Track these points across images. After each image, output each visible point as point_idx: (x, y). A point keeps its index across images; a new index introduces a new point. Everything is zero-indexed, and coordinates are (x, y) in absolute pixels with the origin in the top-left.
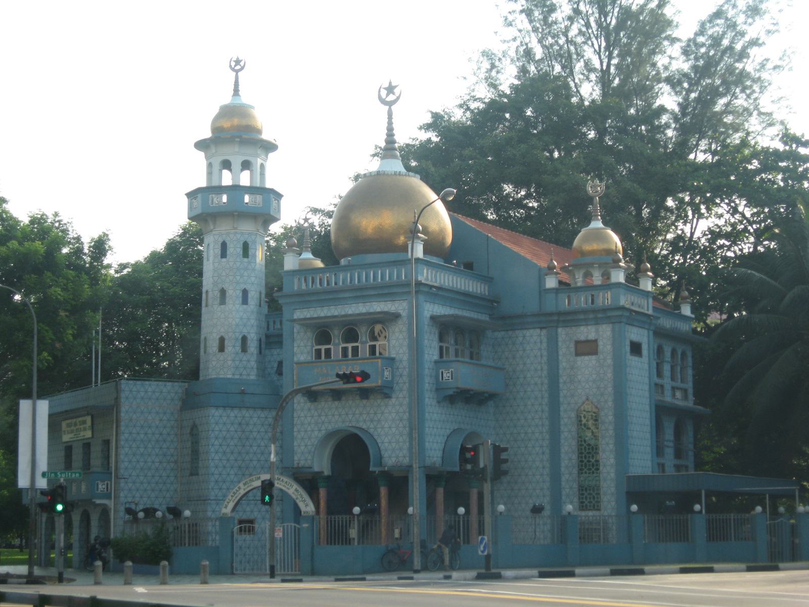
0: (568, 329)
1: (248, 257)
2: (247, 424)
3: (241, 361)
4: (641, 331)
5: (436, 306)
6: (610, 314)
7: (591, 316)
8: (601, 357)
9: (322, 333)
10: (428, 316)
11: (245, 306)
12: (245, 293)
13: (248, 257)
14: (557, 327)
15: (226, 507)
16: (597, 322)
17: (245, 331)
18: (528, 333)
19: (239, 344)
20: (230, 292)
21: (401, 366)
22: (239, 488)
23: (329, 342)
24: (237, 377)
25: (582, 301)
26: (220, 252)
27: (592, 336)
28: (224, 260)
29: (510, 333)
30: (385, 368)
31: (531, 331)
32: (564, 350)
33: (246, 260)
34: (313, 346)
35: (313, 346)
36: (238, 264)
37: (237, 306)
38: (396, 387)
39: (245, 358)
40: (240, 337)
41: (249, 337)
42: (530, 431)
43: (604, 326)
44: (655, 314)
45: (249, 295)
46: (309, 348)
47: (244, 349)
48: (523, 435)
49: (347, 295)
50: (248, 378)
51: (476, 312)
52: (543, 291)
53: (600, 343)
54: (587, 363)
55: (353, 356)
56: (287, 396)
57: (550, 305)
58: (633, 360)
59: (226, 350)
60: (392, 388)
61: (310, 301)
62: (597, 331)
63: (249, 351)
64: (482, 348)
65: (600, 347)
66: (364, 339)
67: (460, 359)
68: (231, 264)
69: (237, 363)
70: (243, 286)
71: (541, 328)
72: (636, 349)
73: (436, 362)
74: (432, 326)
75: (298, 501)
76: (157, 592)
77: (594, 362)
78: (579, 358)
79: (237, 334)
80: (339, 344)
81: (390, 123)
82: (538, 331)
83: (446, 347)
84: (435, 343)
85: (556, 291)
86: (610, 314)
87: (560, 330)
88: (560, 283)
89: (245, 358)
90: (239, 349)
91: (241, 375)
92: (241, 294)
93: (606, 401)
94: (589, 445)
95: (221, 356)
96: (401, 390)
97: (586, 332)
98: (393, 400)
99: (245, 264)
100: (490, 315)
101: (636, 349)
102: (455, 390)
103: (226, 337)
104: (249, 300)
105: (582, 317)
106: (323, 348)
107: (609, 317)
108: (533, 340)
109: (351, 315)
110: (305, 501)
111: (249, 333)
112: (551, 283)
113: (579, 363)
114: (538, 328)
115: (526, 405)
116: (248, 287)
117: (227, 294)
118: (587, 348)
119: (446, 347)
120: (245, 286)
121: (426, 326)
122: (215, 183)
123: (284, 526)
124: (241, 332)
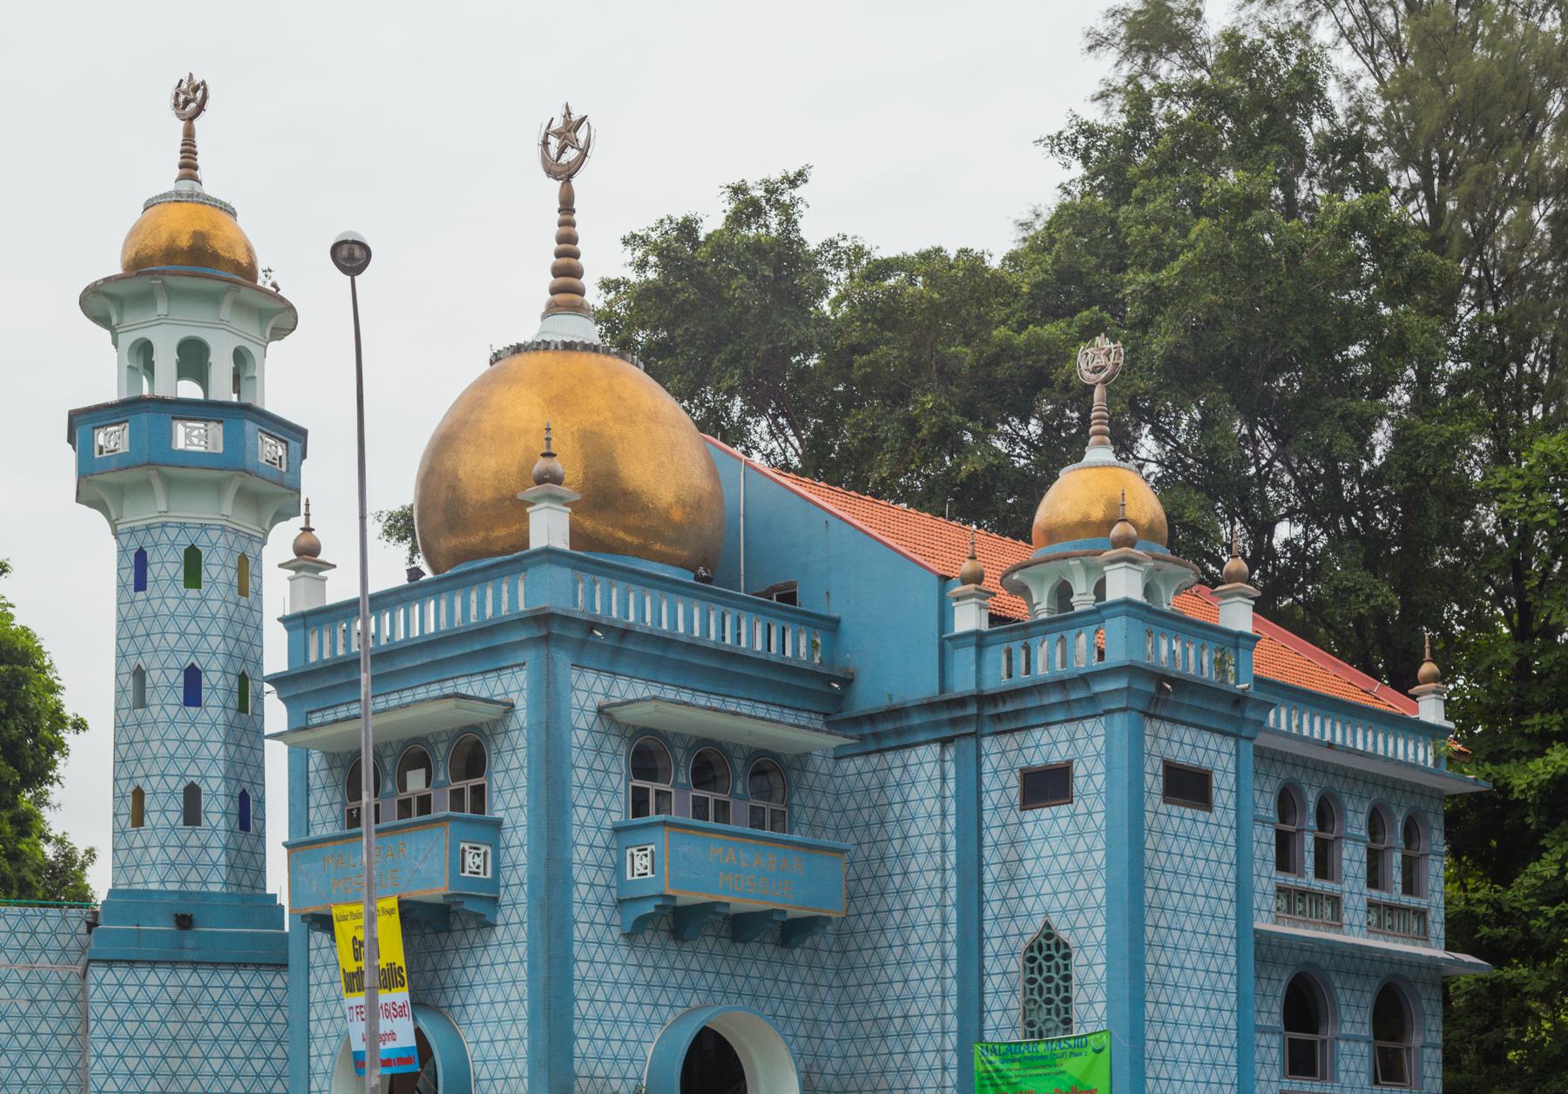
0: (1004, 739)
3: (183, 847)
4: (1213, 741)
5: (622, 683)
8: (1081, 809)
10: (591, 706)
11: (192, 710)
12: (193, 678)
14: (977, 736)
18: (913, 756)
20: (154, 676)
24: (170, 887)
25: (1046, 660)
26: (132, 578)
27: (1056, 758)
28: (141, 595)
29: (874, 759)
30: (467, 846)
33: (193, 593)
36: (172, 603)
37: (172, 710)
38: (505, 898)
40: (181, 787)
41: (204, 787)
42: (914, 1011)
44: (1259, 696)
45: (204, 681)
46: (337, 808)
47: (192, 812)
50: (204, 889)
51: (790, 708)
52: (948, 643)
53: (1079, 771)
54: (1049, 820)
57: (963, 682)
58: (1182, 817)
60: (496, 899)
62: (1072, 740)
63: (204, 822)
64: (796, 799)
65: (1079, 783)
66: (442, 778)
67: (767, 833)
69: (173, 852)
70: (186, 660)
71: (945, 742)
72: (1187, 786)
73: (617, 830)
74: (606, 733)
77: (1063, 822)
78: (1029, 816)
79: (172, 781)
81: (567, 243)
82: (936, 748)
83: (658, 793)
84: (615, 779)
85: (979, 640)
87: (987, 743)
88: (994, 619)
90: (175, 817)
91: (184, 882)
92: (181, 679)
97: (1047, 746)
98: (499, 930)
99: (193, 603)
100: (826, 715)
101: (1187, 786)
102: (659, 902)
103: (147, 789)
104: (205, 694)
108: (924, 776)
111: (203, 777)
112: (968, 618)
113: (1029, 827)
114: (935, 741)
115: (906, 945)
116: (201, 662)
117: (148, 681)
118: (1047, 786)
119: (658, 793)
120: (193, 660)
121: (582, 735)
124: (183, 776)
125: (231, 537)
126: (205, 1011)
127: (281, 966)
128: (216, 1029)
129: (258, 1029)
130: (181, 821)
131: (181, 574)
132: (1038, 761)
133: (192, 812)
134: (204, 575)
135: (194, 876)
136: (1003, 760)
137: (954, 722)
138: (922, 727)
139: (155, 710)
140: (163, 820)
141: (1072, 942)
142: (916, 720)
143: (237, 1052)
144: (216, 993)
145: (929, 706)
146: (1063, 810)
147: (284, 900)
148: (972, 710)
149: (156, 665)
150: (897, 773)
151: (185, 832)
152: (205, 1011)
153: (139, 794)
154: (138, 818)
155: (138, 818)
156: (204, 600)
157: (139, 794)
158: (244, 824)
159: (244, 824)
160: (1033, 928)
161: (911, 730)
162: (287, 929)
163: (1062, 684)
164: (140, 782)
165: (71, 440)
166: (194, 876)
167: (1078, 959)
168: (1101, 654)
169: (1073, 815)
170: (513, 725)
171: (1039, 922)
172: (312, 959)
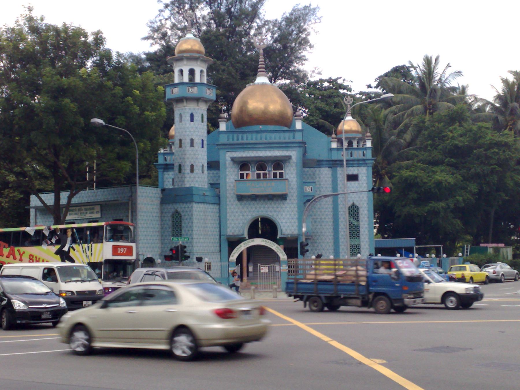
6: (367, 162)
7: (356, 162)
8: (361, 183)
9: (244, 165)
15: (233, 256)
16: (359, 165)
19: (201, 168)
21: (292, 184)
22: (241, 246)
23: (264, 169)
24: (200, 186)
28: (192, 123)
31: (324, 169)
32: (341, 179)
34: (238, 172)
35: (238, 172)
43: (362, 168)
46: (236, 172)
48: (319, 220)
49: (260, 146)
52: (331, 149)
55: (263, 177)
56: (317, 198)
59: (195, 172)
61: (249, 148)
62: (358, 170)
65: (360, 177)
68: (197, 125)
75: (278, 253)
76: (497, 299)
77: (357, 185)
78: (349, 183)
80: (255, 171)
82: (327, 168)
86: (367, 162)
93: (363, 204)
94: (354, 225)
95: (192, 175)
103: (194, 165)
105: (351, 163)
106: (278, 172)
107: (366, 164)
109: (244, 157)
113: (349, 185)
118: (353, 178)
122: (181, 81)
123: (269, 267)
132: (350, 173)
136: (342, 173)
137: (333, 164)
138: (326, 164)
139: (197, 148)
141: (359, 206)
142: (324, 163)
145: (329, 161)
146: (356, 182)
148: (338, 162)
149: (197, 138)
150: (318, 172)
160: (350, 204)
161: (323, 164)
163: (358, 160)
167: (361, 210)
168: (351, 153)
169: (359, 184)
170: (291, 161)
171: (352, 203)
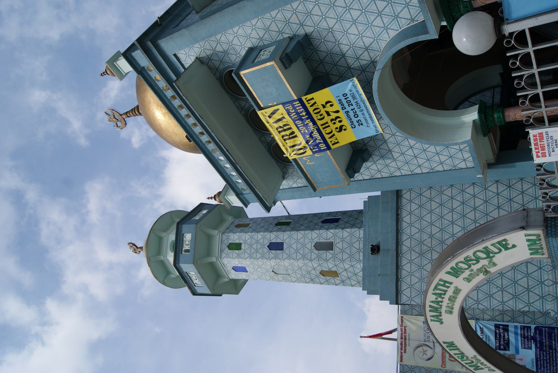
1: (240, 244)
2: (421, 242)
11: (285, 246)
13: (240, 244)
17: (310, 246)
33: (243, 247)
39: (340, 245)
40: (316, 252)
41: (316, 240)
45: (274, 241)
47: (328, 246)
63: (331, 240)
69: (346, 256)
70: (266, 249)
79: (314, 256)
89: (338, 246)
90: (329, 254)
92: (273, 251)
96: (287, 22)
103: (319, 269)
110: (487, 251)
125: (228, 230)
126: (425, 237)
127: (398, 194)
128: (435, 230)
129: (434, 205)
130: (331, 252)
131: (237, 251)
133: (328, 246)
134: (237, 242)
135: (356, 245)
140: (331, 261)
143: (449, 217)
144: (414, 230)
147: (365, 196)
151: (336, 250)
152: (425, 237)
153: (323, 273)
154: (334, 274)
155: (334, 274)
156: (245, 241)
157: (323, 273)
158: (336, 221)
159: (336, 221)
162: (378, 193)
164: (318, 273)
165: (221, 295)
166: (356, 245)
172: (388, 175)
